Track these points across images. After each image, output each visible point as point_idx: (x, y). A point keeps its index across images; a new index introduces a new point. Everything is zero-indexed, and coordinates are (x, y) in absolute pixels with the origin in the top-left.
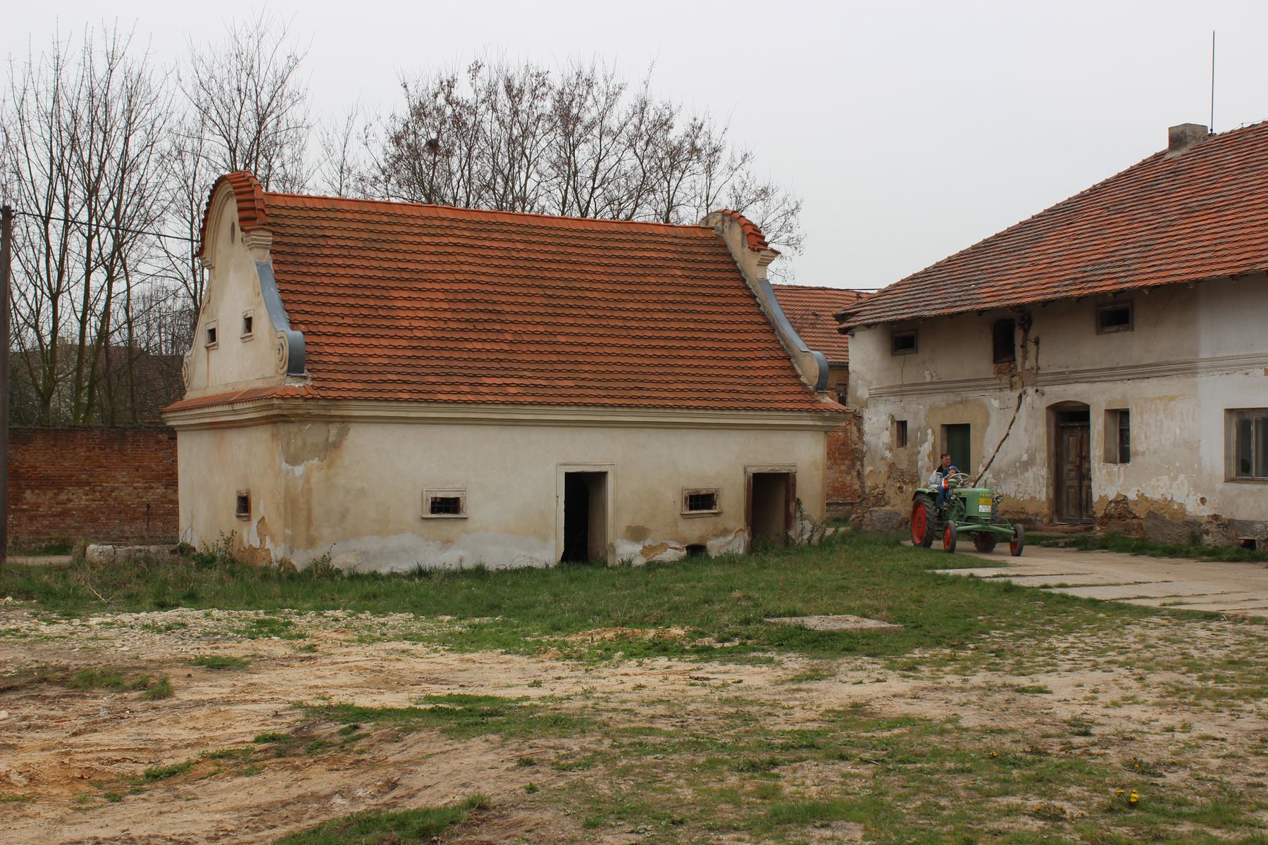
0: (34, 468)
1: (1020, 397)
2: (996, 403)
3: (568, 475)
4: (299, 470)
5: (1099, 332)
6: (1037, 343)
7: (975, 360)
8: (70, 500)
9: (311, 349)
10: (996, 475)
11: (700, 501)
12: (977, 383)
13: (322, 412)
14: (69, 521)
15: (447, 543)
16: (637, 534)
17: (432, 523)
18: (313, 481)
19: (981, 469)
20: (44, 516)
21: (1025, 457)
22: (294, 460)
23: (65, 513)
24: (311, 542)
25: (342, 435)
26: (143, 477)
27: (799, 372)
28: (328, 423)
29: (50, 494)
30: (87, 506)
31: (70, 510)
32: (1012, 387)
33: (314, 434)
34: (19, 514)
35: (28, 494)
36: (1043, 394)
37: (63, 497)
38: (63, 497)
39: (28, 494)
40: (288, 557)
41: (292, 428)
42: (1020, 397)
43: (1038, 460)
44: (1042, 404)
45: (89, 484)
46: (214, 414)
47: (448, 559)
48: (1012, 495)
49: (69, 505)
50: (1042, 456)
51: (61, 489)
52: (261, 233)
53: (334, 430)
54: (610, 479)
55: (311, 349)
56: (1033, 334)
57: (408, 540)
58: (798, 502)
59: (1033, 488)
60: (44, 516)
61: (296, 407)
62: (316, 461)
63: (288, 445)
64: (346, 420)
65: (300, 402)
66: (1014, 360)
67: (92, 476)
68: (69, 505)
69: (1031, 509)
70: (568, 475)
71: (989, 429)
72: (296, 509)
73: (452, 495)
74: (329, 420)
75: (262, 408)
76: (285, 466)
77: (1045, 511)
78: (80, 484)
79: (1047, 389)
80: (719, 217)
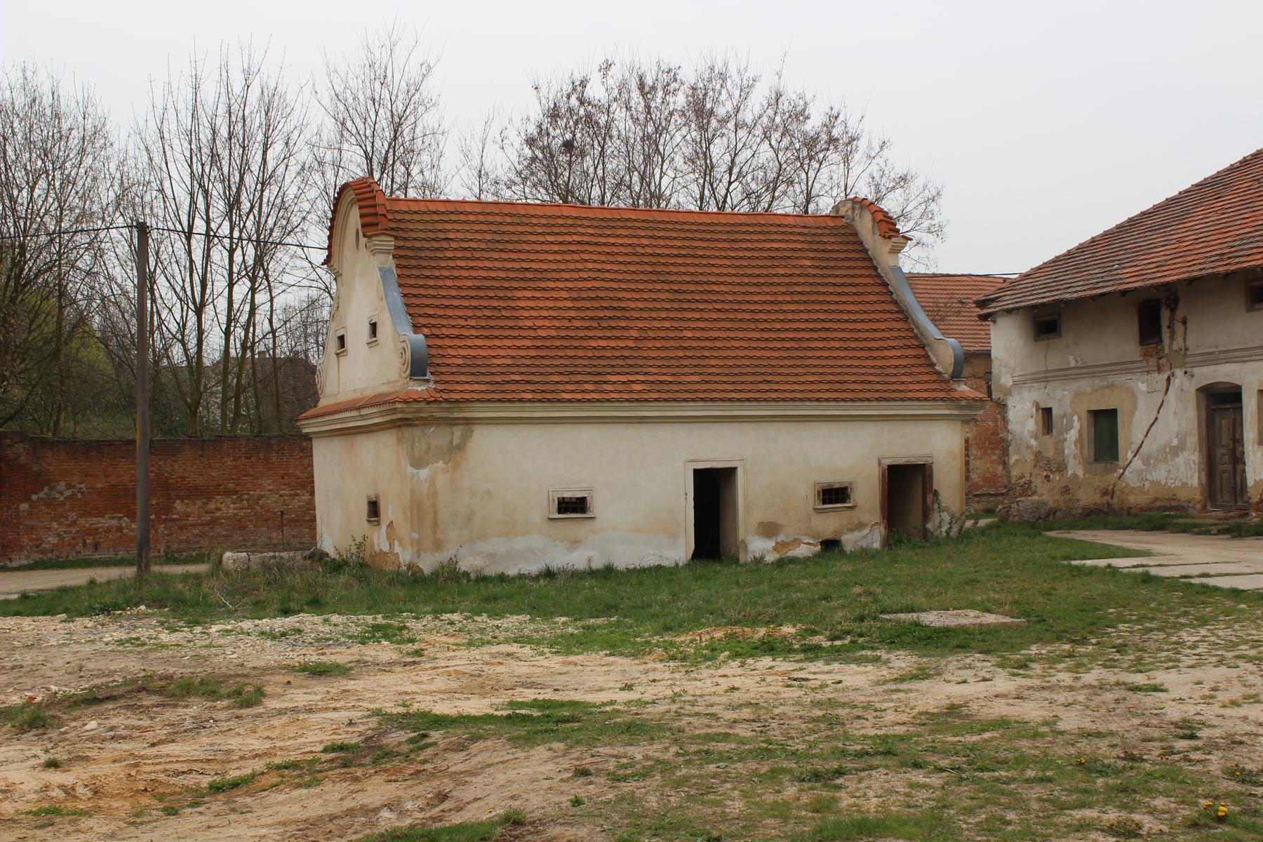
0: (184, 478)
1: (1168, 379)
2: (1143, 387)
3: (695, 471)
4: (424, 473)
5: (1250, 309)
6: (1184, 322)
7: (1121, 342)
8: (219, 509)
9: (433, 352)
10: (1146, 462)
11: (834, 495)
12: (1125, 367)
13: (445, 415)
14: (218, 530)
15: (575, 543)
16: (769, 529)
17: (560, 524)
18: (438, 484)
19: (1130, 455)
20: (194, 526)
21: (1175, 442)
22: (418, 463)
23: (213, 522)
24: (438, 545)
25: (466, 438)
26: (289, 485)
27: (934, 360)
28: (451, 425)
29: (199, 503)
30: (235, 515)
31: (218, 518)
32: (1159, 369)
33: (438, 437)
34: (170, 524)
35: (178, 504)
36: (1192, 376)
37: (212, 506)
38: (212, 506)
39: (178, 504)
40: (415, 560)
41: (417, 432)
42: (1168, 379)
43: (1189, 445)
44: (1191, 386)
45: (236, 492)
46: (343, 420)
47: (578, 559)
48: (1163, 482)
49: (218, 514)
50: (1193, 440)
51: (209, 498)
52: (383, 238)
53: (458, 432)
54: (740, 474)
55: (433, 352)
56: (1180, 314)
57: (535, 541)
58: (936, 494)
59: (1184, 473)
60: (194, 526)
61: (419, 411)
62: (441, 464)
63: (413, 449)
64: (469, 422)
65: (423, 405)
66: (1161, 341)
67: (239, 484)
68: (218, 514)
69: (1183, 496)
70: (695, 471)
71: (1137, 414)
72: (423, 511)
73: (579, 495)
74: (452, 422)
75: (381, 414)
76: (410, 469)
77: (1198, 497)
78: (228, 493)
79: (1196, 370)
80: (849, 205)
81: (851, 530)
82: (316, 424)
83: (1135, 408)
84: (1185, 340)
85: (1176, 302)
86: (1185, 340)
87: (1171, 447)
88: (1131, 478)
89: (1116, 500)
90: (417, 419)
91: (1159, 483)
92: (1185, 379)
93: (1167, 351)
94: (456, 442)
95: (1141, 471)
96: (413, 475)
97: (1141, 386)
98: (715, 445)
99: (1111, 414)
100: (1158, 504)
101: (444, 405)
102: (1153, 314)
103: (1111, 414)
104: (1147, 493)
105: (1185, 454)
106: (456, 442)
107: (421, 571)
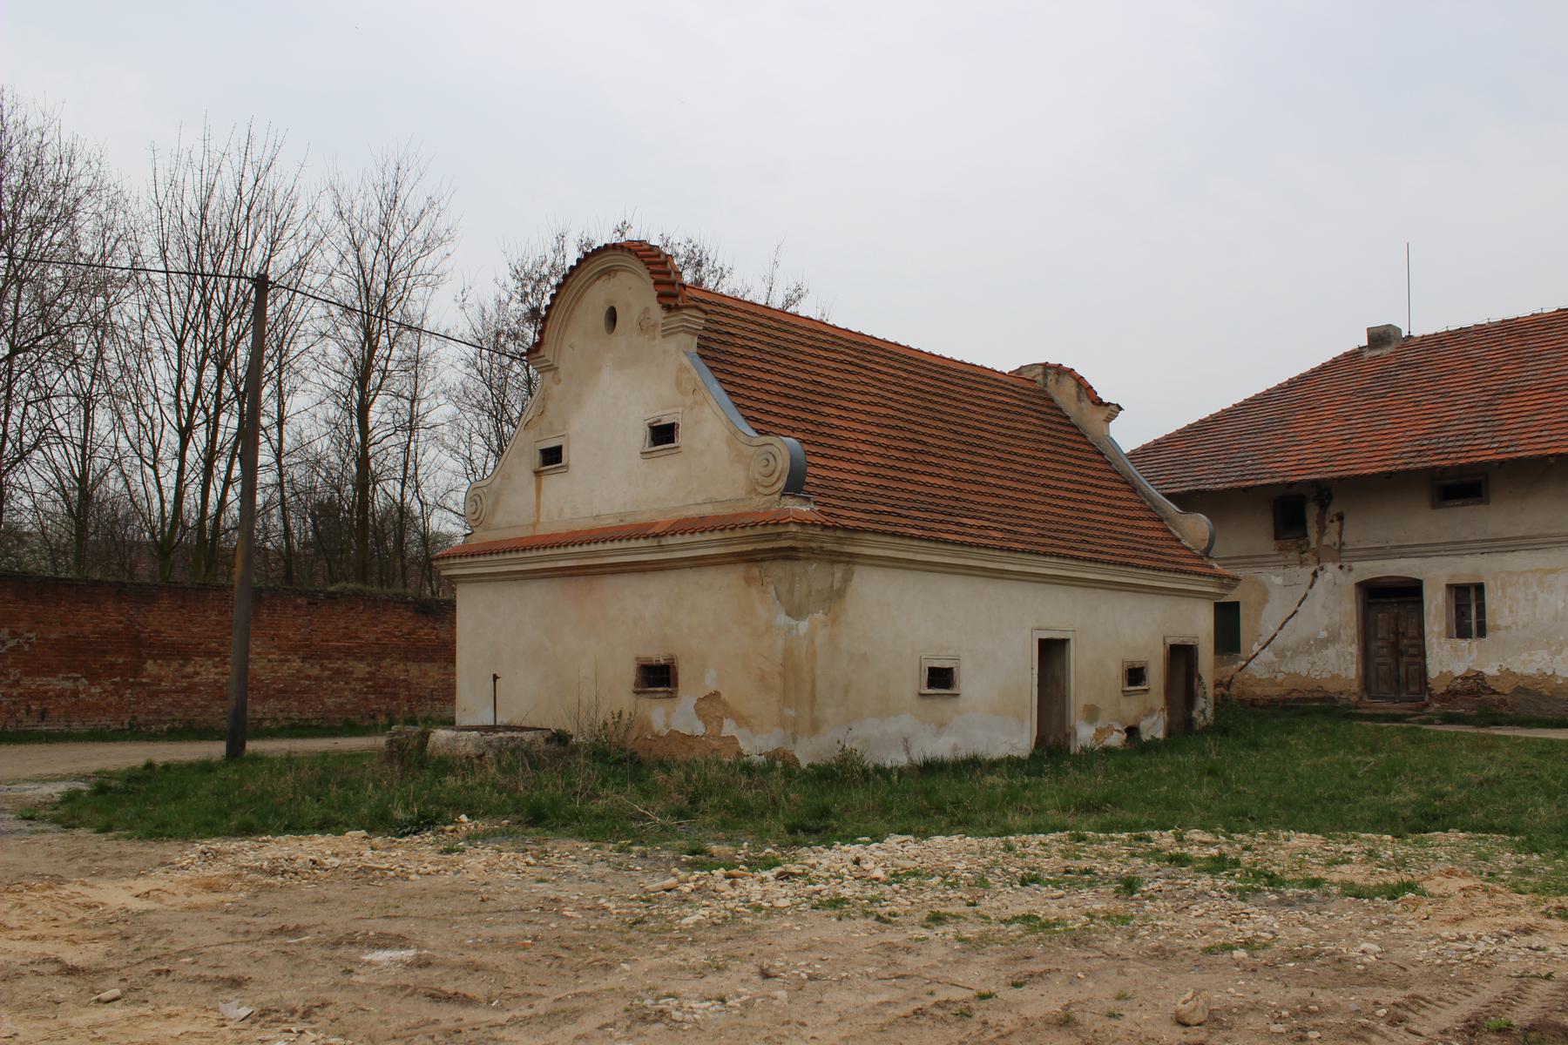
0: (158, 632)
1: (1315, 574)
2: (1278, 581)
3: (1041, 641)
4: (803, 626)
5: (1434, 506)
6: (1340, 517)
7: (1254, 536)
8: (197, 673)
9: (810, 459)
10: (1281, 654)
11: (1135, 675)
12: (1258, 561)
13: (835, 547)
14: (195, 698)
15: (941, 726)
16: (1092, 713)
17: (928, 701)
18: (818, 641)
19: (1256, 647)
20: (167, 692)
21: (1324, 634)
22: (796, 612)
23: (190, 689)
24: (815, 727)
25: (847, 580)
26: (279, 648)
27: (1178, 535)
28: (833, 562)
29: (175, 665)
30: (216, 681)
31: (196, 685)
32: (1302, 563)
33: (816, 577)
34: (138, 689)
35: (150, 666)
36: (1350, 570)
37: (190, 669)
38: (190, 669)
39: (150, 666)
40: (789, 747)
41: (797, 567)
42: (1315, 574)
43: (1343, 637)
44: (1349, 581)
45: (219, 654)
46: (596, 554)
47: (942, 747)
48: (1304, 674)
49: (197, 680)
50: (1350, 631)
51: (187, 659)
52: (694, 312)
53: (839, 571)
54: (1073, 651)
55: (810, 459)
56: (1333, 509)
57: (904, 724)
58: (1200, 678)
59: (1339, 664)
60: (167, 692)
61: (812, 538)
62: (820, 615)
63: (791, 591)
64: (852, 559)
65: (818, 531)
66: (1306, 535)
67: (223, 644)
68: (197, 680)
69: (1332, 688)
70: (1041, 641)
71: (1268, 607)
72: (793, 679)
73: (947, 665)
74: (835, 558)
75: (764, 538)
76: (782, 619)
77: (1355, 688)
78: (209, 654)
79: (1355, 565)
80: (1040, 370)
81: (1146, 716)
82: (463, 566)
83: (1265, 599)
84: (1340, 535)
85: (1330, 498)
86: (1340, 535)
87: (1316, 640)
88: (1257, 669)
89: (1233, 691)
90: (806, 550)
91: (1299, 675)
92: (1339, 573)
93: (1313, 545)
94: (837, 585)
95: (1273, 663)
96: (791, 628)
97: (1275, 579)
98: (1058, 610)
99: (1234, 607)
100: (1295, 695)
101: (839, 534)
102: (1294, 513)
103: (1234, 607)
104: (1281, 685)
105: (1338, 646)
106: (837, 585)
107: (796, 761)
